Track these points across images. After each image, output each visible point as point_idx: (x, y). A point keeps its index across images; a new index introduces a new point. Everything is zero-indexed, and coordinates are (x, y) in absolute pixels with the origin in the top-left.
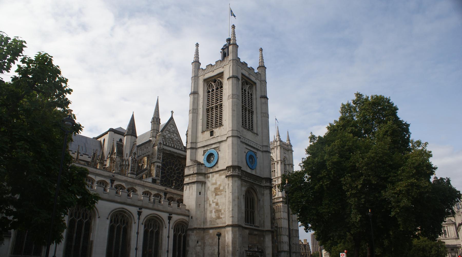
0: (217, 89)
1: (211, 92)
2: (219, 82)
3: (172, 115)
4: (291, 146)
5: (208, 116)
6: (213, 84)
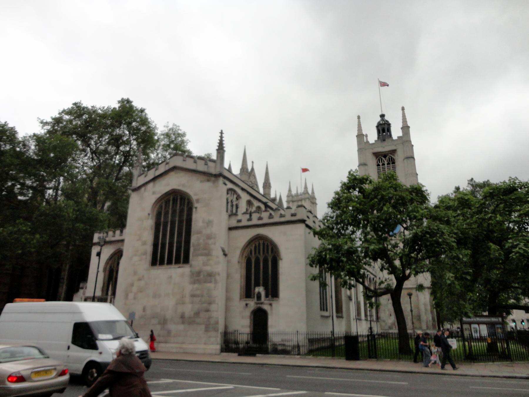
0: (388, 164)
2: (390, 158)
3: (253, 165)
4: (315, 199)
6: (384, 159)
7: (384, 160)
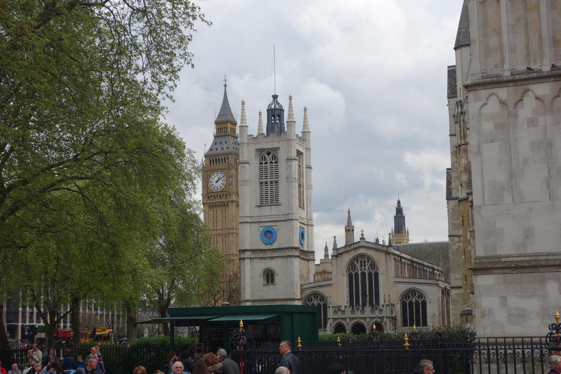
0: (271, 163)
1: (264, 164)
5: (261, 189)
6: (267, 156)
7: (268, 158)
